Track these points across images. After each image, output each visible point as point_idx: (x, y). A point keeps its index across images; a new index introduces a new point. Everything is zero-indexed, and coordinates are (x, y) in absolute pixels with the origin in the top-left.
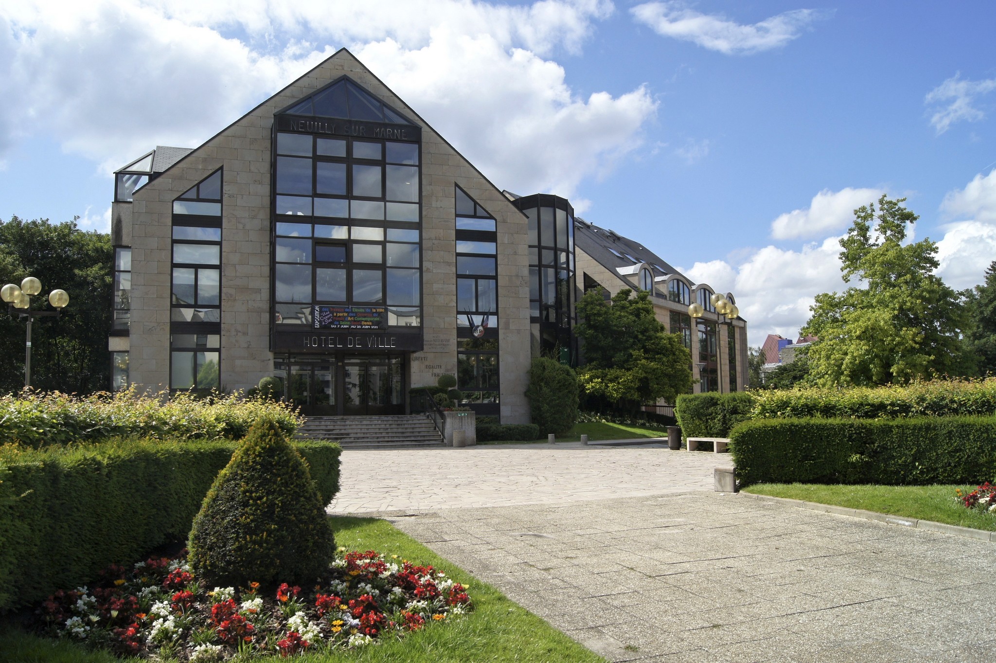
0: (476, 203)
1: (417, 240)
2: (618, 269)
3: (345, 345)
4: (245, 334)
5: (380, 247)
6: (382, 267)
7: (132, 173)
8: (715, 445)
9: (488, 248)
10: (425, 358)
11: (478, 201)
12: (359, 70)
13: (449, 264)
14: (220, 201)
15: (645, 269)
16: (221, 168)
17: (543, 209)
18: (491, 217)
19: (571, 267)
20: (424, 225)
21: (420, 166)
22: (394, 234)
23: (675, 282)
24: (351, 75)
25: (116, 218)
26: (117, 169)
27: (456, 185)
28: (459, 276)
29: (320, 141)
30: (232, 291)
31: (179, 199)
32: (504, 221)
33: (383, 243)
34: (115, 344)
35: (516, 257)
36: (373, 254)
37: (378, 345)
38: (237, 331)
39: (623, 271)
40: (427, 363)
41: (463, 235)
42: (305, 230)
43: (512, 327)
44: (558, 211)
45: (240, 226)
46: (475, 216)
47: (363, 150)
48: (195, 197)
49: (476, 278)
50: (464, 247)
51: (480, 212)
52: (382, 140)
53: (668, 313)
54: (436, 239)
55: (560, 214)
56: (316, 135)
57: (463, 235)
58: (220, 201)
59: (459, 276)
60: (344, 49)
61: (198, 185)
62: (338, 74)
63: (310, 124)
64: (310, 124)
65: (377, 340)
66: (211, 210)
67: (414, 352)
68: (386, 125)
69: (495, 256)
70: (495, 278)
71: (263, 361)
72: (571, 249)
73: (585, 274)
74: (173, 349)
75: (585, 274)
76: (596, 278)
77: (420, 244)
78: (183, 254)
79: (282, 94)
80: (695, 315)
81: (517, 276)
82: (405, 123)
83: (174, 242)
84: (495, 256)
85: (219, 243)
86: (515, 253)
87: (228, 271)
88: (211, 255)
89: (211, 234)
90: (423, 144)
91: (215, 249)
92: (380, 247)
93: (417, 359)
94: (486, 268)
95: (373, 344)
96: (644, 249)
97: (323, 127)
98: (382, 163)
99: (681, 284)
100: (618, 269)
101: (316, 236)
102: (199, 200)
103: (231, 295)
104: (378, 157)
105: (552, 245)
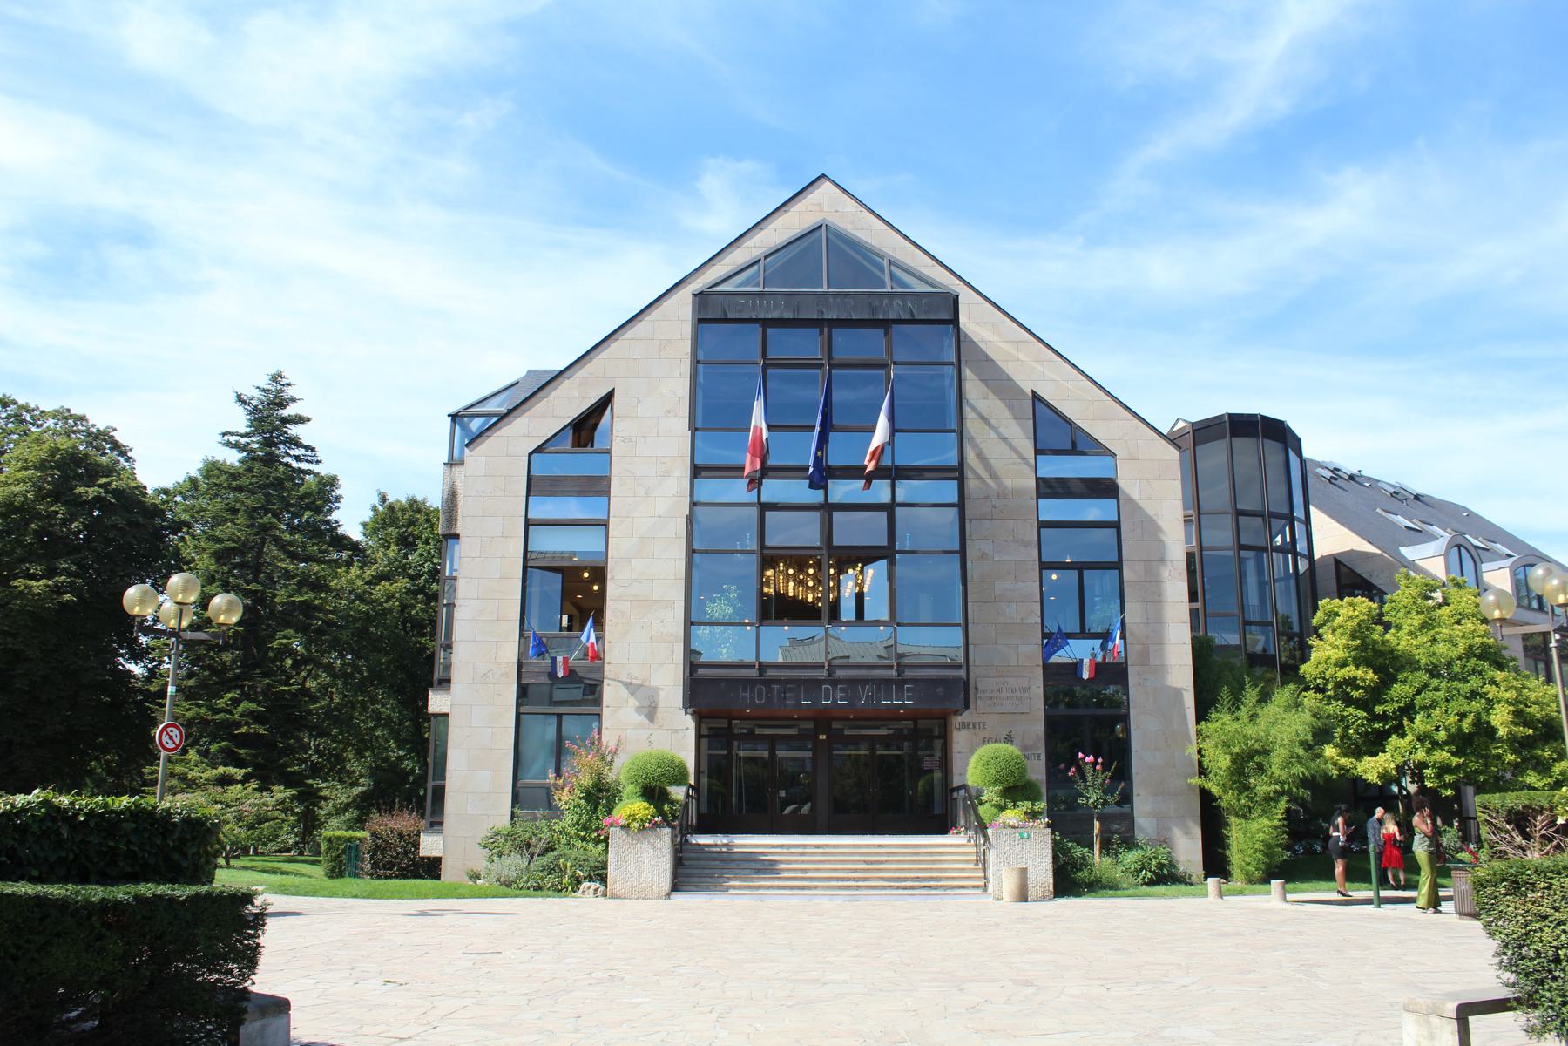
1: (954, 499)
2: (1403, 550)
3: (816, 701)
10: (983, 725)
13: (1024, 543)
15: (1459, 546)
17: (1237, 442)
19: (1301, 546)
22: (906, 490)
25: (447, 488)
26: (453, 410)
33: (890, 508)
36: (869, 530)
37: (879, 700)
41: (1050, 488)
54: (998, 497)
55: (1272, 447)
57: (1050, 488)
59: (1045, 566)
63: (754, 303)
64: (754, 303)
65: (879, 690)
67: (957, 713)
69: (1116, 526)
70: (1117, 566)
71: (677, 731)
72: (1299, 513)
77: (961, 505)
84: (1116, 526)
93: (965, 726)
94: (1097, 545)
96: (1471, 515)
97: (776, 306)
100: (1403, 550)
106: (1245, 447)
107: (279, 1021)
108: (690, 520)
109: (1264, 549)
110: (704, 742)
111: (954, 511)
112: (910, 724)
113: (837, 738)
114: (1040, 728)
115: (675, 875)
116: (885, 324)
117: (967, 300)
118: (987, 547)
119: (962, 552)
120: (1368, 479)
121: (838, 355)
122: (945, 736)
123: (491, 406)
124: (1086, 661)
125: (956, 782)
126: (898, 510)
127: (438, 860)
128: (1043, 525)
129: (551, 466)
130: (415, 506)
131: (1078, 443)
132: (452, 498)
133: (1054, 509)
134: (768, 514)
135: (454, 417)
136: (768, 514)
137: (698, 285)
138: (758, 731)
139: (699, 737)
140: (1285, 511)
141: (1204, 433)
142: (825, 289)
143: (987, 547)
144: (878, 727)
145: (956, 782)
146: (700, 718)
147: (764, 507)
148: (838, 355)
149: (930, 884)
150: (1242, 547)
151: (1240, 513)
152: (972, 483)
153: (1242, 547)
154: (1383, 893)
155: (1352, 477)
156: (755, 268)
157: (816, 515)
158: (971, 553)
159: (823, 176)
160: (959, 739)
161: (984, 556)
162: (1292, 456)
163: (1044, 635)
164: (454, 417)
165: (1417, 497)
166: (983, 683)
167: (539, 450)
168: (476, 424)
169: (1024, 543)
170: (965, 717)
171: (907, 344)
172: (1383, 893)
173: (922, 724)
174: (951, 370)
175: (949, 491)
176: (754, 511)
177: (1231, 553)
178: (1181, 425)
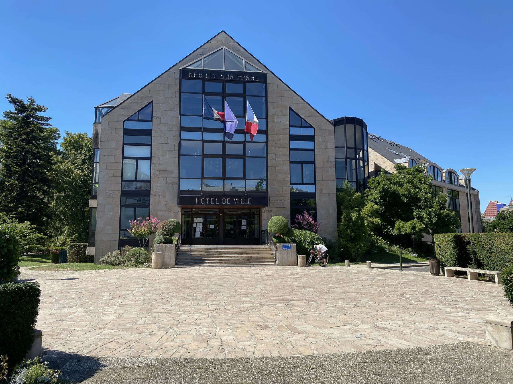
1: (265, 141)
4: (164, 197)
5: (242, 145)
6: (243, 157)
8: (469, 274)
9: (308, 145)
11: (303, 117)
13: (285, 155)
15: (412, 160)
16: (152, 102)
17: (348, 126)
18: (311, 127)
19: (366, 159)
23: (432, 167)
27: (290, 108)
30: (157, 173)
32: (320, 129)
33: (244, 143)
34: (93, 203)
35: (326, 150)
36: (238, 149)
38: (160, 196)
39: (398, 161)
41: (293, 138)
42: (197, 135)
43: (325, 192)
44: (357, 126)
45: (163, 135)
47: (231, 88)
48: (137, 119)
49: (302, 163)
54: (277, 140)
55: (358, 128)
57: (293, 138)
58: (151, 121)
59: (291, 162)
60: (223, 31)
69: (314, 150)
70: (314, 163)
73: (375, 163)
75: (375, 163)
76: (382, 166)
77: (266, 142)
81: (328, 161)
86: (326, 148)
87: (154, 161)
91: (148, 148)
92: (242, 145)
93: (266, 211)
99: (436, 169)
101: (204, 139)
102: (139, 120)
103: (157, 175)
104: (241, 92)
106: (350, 128)
107: (39, 338)
108: (180, 145)
109: (352, 159)
110: (183, 216)
112: (248, 211)
113: (225, 214)
114: (289, 212)
116: (244, 82)
117: (269, 75)
118: (274, 156)
120: (383, 139)
122: (259, 215)
125: (263, 228)
127: (93, 256)
129: (131, 125)
130: (81, 138)
131: (302, 123)
132: (96, 136)
133: (296, 144)
135: (97, 108)
136: (206, 144)
138: (200, 212)
139: (182, 214)
141: (337, 123)
142: (224, 70)
143: (274, 156)
144: (238, 211)
147: (204, 141)
150: (347, 158)
151: (347, 148)
153: (347, 158)
154: (403, 265)
155: (378, 138)
156: (200, 62)
158: (269, 158)
160: (264, 215)
161: (272, 159)
162: (364, 130)
164: (97, 108)
165: (397, 145)
166: (271, 198)
167: (127, 120)
168: (104, 111)
169: (285, 155)
170: (267, 208)
172: (403, 265)
173: (252, 210)
174: (264, 98)
177: (344, 160)
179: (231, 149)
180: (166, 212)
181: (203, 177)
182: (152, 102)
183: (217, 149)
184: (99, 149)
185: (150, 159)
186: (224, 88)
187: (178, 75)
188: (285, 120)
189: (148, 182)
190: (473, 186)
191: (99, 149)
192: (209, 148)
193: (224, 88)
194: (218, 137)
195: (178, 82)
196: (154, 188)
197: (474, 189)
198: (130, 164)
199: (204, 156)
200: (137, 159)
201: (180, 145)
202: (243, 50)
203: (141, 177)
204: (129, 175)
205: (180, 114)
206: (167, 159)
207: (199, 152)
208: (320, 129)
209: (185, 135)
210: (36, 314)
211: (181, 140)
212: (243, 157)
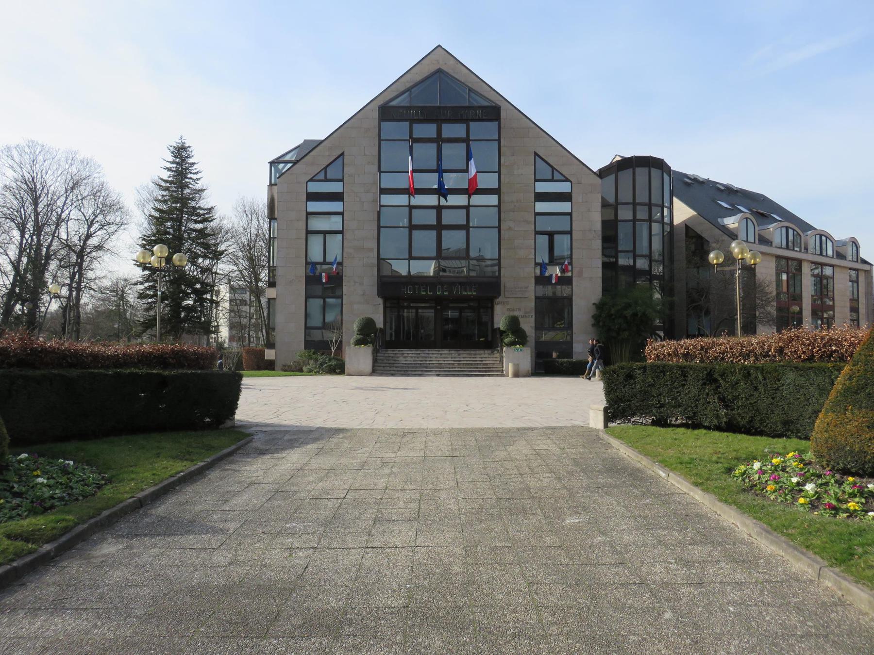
0: (553, 169)
1: (496, 203)
5: (464, 211)
7: (287, 162)
9: (565, 207)
10: (507, 303)
12: (452, 61)
13: (528, 222)
14: (342, 180)
15: (747, 218)
16: (343, 154)
17: (639, 170)
18: (567, 180)
19: (666, 220)
20: (503, 189)
21: (499, 141)
22: (477, 200)
23: (784, 230)
24: (444, 68)
26: (271, 159)
27: (536, 154)
28: (537, 233)
29: (415, 126)
31: (311, 180)
32: (579, 183)
33: (467, 208)
36: (458, 218)
38: (355, 282)
40: (508, 307)
42: (403, 200)
44: (653, 170)
46: (552, 180)
47: (452, 130)
50: (541, 207)
51: (557, 176)
52: (466, 121)
53: (774, 259)
55: (655, 173)
56: (412, 121)
60: (439, 46)
61: (325, 168)
62: (434, 68)
66: (334, 187)
68: (469, 108)
70: (570, 233)
74: (307, 297)
78: (318, 224)
79: (389, 90)
80: (715, 262)
82: (486, 104)
83: (308, 214)
84: (570, 214)
85: (341, 214)
87: (347, 235)
88: (335, 223)
89: (336, 206)
90: (502, 121)
91: (338, 219)
92: (464, 211)
93: (499, 303)
94: (561, 224)
95: (458, 291)
97: (417, 113)
98: (466, 140)
99: (791, 231)
101: (412, 204)
102: (326, 180)
104: (463, 135)
105: (647, 201)
108: (379, 213)
111: (496, 209)
115: (374, 366)
119: (499, 227)
121: (445, 135)
123: (287, 158)
124: (554, 275)
126: (471, 209)
128: (537, 214)
129: (314, 187)
134: (413, 210)
136: (413, 210)
137: (381, 102)
139: (385, 308)
140: (660, 203)
145: (496, 326)
146: (386, 299)
147: (411, 208)
148: (445, 135)
149: (485, 371)
152: (505, 197)
157: (435, 211)
159: (439, 46)
161: (510, 228)
162: (665, 175)
163: (536, 264)
169: (528, 222)
170: (500, 299)
171: (479, 129)
175: (493, 200)
176: (407, 209)
178: (618, 158)
179: (448, 218)
180: (361, 303)
181: (411, 258)
182: (343, 154)
183: (431, 218)
184: (275, 219)
185: (341, 232)
186: (439, 131)
187: (376, 115)
188: (528, 172)
189: (340, 264)
190: (863, 254)
191: (275, 219)
192: (420, 217)
193: (439, 131)
194: (431, 200)
195: (376, 123)
196: (347, 272)
197: (865, 262)
198: (316, 244)
199: (412, 227)
200: (325, 233)
201: (379, 213)
202: (468, 71)
203: (330, 258)
204: (316, 255)
205: (380, 171)
206: (363, 233)
207: (406, 222)
208: (579, 183)
209: (387, 200)
210: (238, 399)
211: (380, 206)
212: (466, 227)
